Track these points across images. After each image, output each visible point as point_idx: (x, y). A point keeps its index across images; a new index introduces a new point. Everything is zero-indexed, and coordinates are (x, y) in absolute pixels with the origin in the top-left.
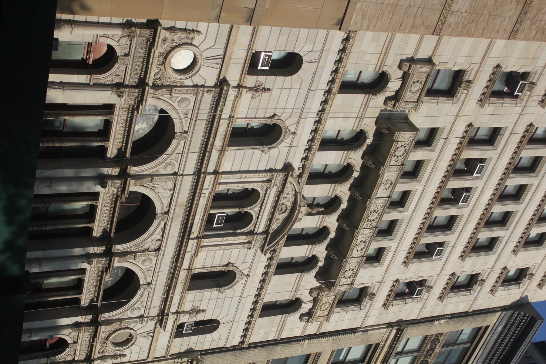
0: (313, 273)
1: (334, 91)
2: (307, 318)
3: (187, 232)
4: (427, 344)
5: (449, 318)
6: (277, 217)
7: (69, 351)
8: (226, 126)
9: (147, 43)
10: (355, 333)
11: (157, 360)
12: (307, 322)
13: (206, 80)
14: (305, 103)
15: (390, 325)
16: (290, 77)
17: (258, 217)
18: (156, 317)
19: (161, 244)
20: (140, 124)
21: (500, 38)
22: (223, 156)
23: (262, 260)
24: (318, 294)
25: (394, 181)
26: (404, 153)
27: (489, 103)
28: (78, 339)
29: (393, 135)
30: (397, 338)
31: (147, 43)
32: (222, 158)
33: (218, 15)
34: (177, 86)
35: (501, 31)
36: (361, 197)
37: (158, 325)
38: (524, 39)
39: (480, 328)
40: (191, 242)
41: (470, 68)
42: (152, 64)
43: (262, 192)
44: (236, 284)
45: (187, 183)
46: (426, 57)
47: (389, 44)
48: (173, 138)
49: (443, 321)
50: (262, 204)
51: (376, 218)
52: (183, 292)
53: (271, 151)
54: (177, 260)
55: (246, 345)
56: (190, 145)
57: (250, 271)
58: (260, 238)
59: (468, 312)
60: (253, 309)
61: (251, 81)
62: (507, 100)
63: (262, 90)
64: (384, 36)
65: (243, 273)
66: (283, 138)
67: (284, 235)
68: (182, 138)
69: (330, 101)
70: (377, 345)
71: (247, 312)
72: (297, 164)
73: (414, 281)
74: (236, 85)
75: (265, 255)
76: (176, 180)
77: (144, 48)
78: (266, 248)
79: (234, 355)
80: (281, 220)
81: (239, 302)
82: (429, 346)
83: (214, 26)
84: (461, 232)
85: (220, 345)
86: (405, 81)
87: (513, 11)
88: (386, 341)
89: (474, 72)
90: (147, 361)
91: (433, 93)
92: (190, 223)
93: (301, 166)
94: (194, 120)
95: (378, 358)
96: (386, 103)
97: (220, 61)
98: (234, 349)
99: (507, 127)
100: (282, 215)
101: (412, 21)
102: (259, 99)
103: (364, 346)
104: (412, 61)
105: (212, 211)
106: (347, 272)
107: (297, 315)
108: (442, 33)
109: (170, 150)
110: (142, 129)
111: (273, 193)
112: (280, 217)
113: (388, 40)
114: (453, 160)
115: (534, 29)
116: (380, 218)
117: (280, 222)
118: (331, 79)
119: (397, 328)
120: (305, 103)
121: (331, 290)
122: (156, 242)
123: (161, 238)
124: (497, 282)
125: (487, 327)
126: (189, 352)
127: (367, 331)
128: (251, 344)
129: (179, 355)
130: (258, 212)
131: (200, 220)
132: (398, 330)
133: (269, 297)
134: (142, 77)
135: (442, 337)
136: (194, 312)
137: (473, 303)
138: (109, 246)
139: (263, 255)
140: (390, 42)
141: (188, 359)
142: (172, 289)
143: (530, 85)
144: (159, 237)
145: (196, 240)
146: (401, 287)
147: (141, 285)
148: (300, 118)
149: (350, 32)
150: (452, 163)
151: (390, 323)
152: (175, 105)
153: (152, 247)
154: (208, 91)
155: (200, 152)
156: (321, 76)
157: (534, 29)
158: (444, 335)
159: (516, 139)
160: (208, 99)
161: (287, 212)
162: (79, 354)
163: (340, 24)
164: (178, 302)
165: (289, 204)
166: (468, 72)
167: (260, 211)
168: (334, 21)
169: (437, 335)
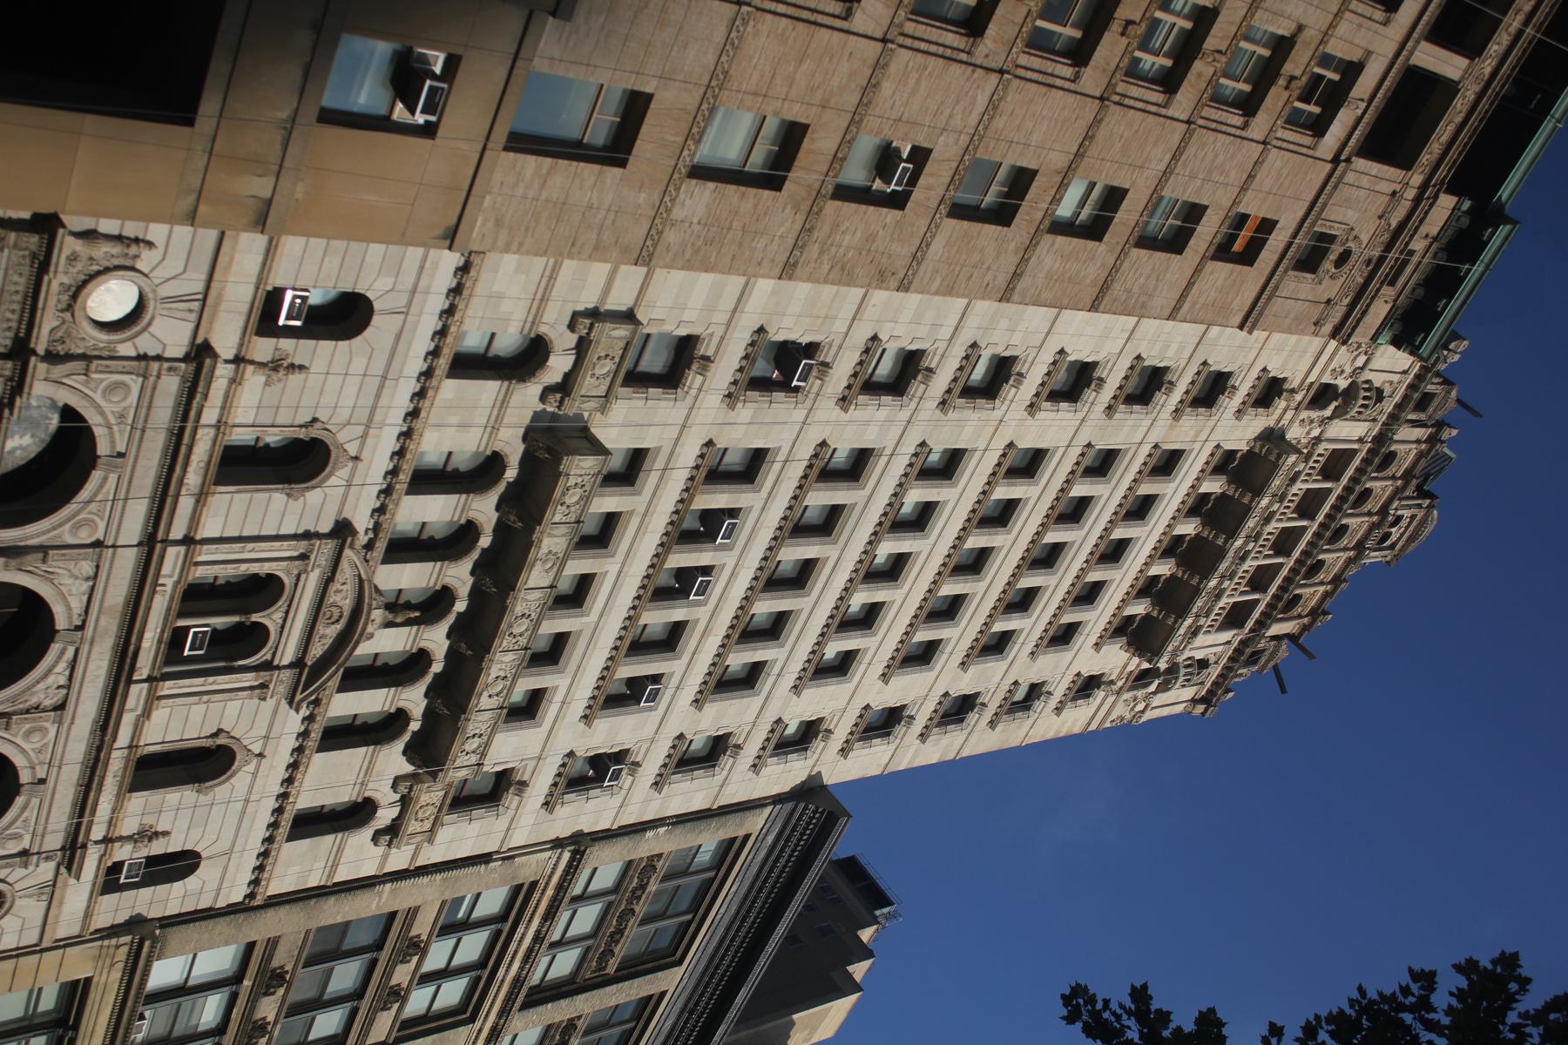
0: (400, 745)
1: (438, 372)
2: (388, 838)
4: (632, 877)
5: (673, 824)
6: (321, 632)
8: (210, 443)
9: (33, 263)
10: (487, 863)
11: (62, 943)
12: (389, 845)
13: (165, 345)
14: (378, 396)
15: (558, 844)
16: (346, 343)
17: (281, 633)
18: (59, 853)
19: (67, 694)
20: (16, 437)
21: (763, 276)
22: (204, 505)
23: (293, 722)
24: (411, 788)
25: (561, 555)
26: (581, 498)
27: (745, 401)
29: (559, 461)
30: (572, 869)
31: (33, 263)
32: (202, 510)
33: (192, 209)
34: (100, 358)
35: (765, 263)
37: (63, 870)
38: (808, 280)
39: (734, 839)
40: (134, 689)
41: (708, 331)
42: (44, 309)
43: (288, 581)
44: (235, 773)
45: (125, 565)
46: (624, 308)
47: (549, 281)
48: (93, 466)
49: (662, 830)
51: (527, 630)
52: (118, 796)
53: (308, 494)
54: (104, 728)
55: (259, 901)
57: (265, 745)
58: (287, 675)
59: (709, 810)
60: (274, 825)
61: (263, 348)
62: (779, 396)
63: (287, 367)
64: (539, 264)
65: (249, 750)
66: (333, 468)
67: (337, 670)
68: (112, 467)
69: (430, 393)
70: (534, 885)
71: (261, 832)
72: (362, 521)
73: (605, 753)
74: (231, 357)
75: (297, 711)
78: (298, 697)
81: (244, 812)
82: (636, 880)
83: (183, 232)
84: (694, 654)
87: (787, 225)
88: (550, 877)
89: (715, 340)
90: (38, 948)
91: (637, 379)
92: (132, 648)
93: (371, 526)
94: (140, 429)
95: (534, 911)
97: (196, 306)
98: (233, 910)
99: (780, 448)
100: (333, 627)
101: (594, 236)
102: (280, 386)
103: (508, 887)
104: (595, 314)
105: (181, 623)
107: (367, 833)
108: (653, 262)
109: (87, 493)
110: (21, 448)
111: (313, 580)
112: (328, 633)
113: (547, 273)
114: (676, 512)
115: (826, 262)
117: (328, 641)
118: (431, 348)
119: (572, 848)
120: (378, 396)
123: (67, 683)
124: (763, 748)
125: (747, 837)
126: (135, 924)
127: (512, 857)
128: (270, 897)
129: (113, 931)
130: (280, 621)
131: (155, 642)
132: (574, 853)
133: (307, 798)
134: (21, 335)
135: (661, 863)
136: (143, 837)
137: (719, 791)
139: (293, 712)
140: (552, 277)
143: (821, 368)
144: (62, 680)
145: (146, 685)
146: (578, 767)
147: (23, 785)
148: (368, 426)
149: (470, 253)
150: (675, 517)
151: (558, 839)
152: (98, 397)
153: (48, 703)
154: (170, 369)
155: (153, 498)
156: (410, 344)
157: (826, 262)
158: (664, 856)
159: (796, 470)
160: (171, 385)
161: (343, 621)
163: (451, 237)
165: (347, 604)
166: (704, 339)
167: (285, 620)
168: (439, 231)
169: (651, 858)
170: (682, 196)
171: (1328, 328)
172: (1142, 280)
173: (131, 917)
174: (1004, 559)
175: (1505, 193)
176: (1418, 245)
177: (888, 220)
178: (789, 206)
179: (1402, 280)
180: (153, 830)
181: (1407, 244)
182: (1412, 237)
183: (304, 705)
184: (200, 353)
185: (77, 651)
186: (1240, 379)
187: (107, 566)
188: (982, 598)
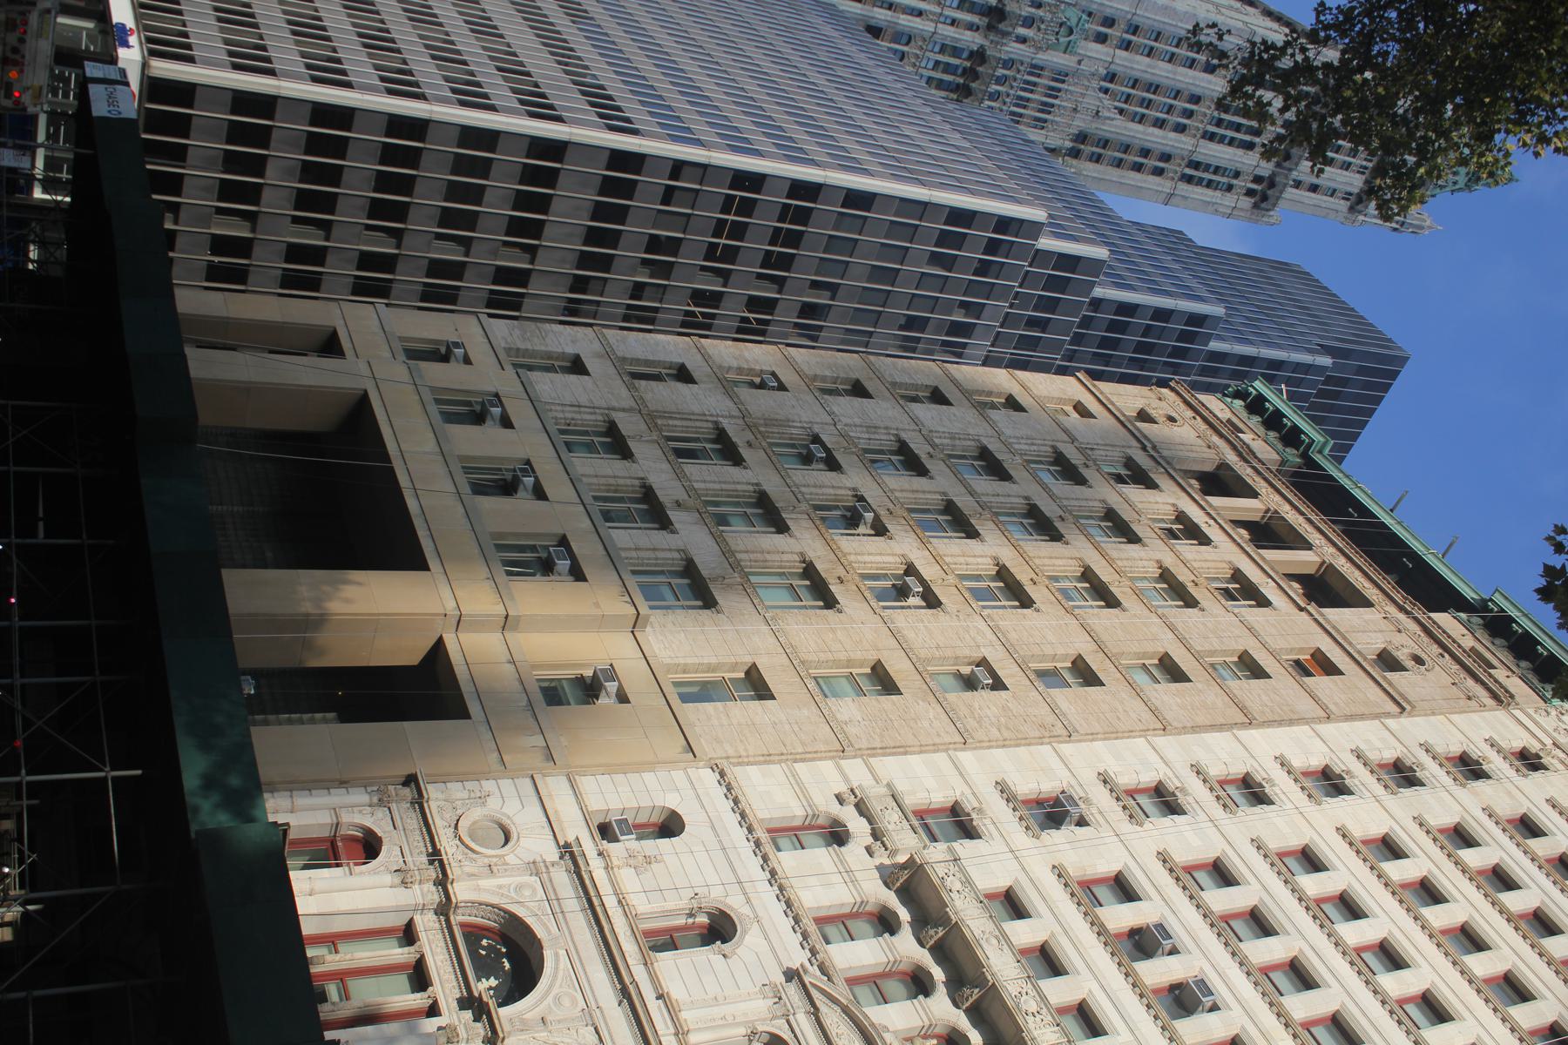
22: (652, 964)
43: (786, 1035)
56: (577, 952)
76: (592, 1017)
77: (414, 815)
83: (506, 784)
93: (719, 777)
110: (490, 988)
113: (789, 774)
116: (1045, 1004)
150: (1096, 929)
170: (833, 708)
171: (1490, 702)
172: (1264, 698)
174: (1493, 928)
175: (1469, 594)
176: (1468, 642)
178: (920, 702)
179: (1488, 655)
181: (1464, 651)
182: (1460, 646)
184: (568, 852)
186: (1476, 751)
187: (603, 1025)
188: (1522, 959)
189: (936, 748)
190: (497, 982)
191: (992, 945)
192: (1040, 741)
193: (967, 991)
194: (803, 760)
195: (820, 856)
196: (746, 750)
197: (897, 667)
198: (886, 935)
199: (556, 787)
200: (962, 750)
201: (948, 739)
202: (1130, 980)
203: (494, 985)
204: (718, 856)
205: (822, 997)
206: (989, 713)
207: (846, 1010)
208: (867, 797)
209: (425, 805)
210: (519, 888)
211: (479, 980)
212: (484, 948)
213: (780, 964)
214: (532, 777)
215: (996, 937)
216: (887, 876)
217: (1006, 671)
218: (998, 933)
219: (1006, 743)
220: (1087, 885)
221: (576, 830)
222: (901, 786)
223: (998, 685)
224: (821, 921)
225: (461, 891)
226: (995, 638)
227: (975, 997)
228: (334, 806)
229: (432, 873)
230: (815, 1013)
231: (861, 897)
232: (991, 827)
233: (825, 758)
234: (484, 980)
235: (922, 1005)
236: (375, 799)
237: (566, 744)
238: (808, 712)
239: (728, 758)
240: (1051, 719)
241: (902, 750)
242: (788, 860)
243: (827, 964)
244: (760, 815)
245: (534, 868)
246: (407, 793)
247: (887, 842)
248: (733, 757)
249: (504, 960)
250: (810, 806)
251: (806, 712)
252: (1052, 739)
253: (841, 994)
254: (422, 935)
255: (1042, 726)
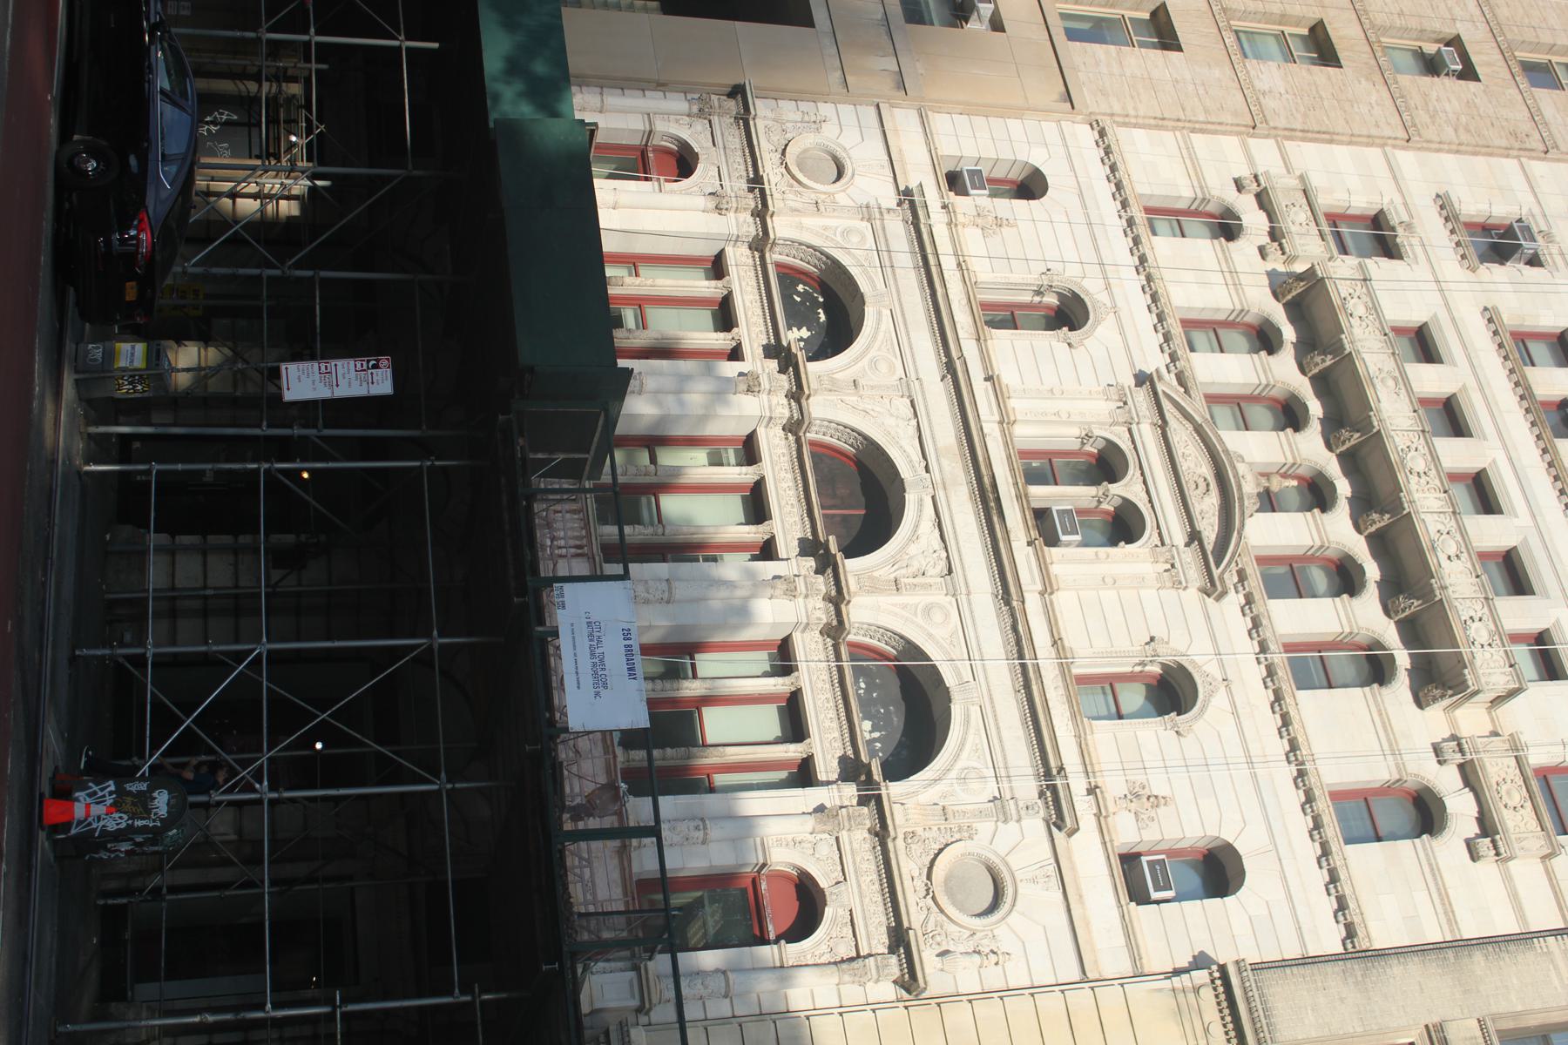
0: (1401, 686)
1: (1257, 596)
3: (992, 504)
7: (834, 920)
17: (1153, 507)
19: (948, 557)
22: (985, 340)
28: (844, 874)
36: (1358, 431)
43: (1125, 445)
50: (1143, 474)
54: (1006, 597)
56: (903, 315)
69: (1308, 766)
77: (737, 132)
78: (1216, 573)
79: (1350, 980)
80: (1214, 515)
81: (1254, 776)
83: (846, 110)
85: (1292, 952)
86: (1270, 208)
92: (986, 480)
96: (1475, 855)
106: (1475, 626)
110: (801, 339)
111: (1148, 436)
112: (1207, 508)
113: (1182, 145)
116: (1435, 465)
121: (1466, 681)
122: (935, 555)
131: (1015, 499)
138: (821, 552)
141: (1211, 974)
142: (1033, 682)
150: (1520, 391)
162: (866, 926)
164: (1081, 768)
165: (1206, 470)
167: (1148, 492)
168: (1055, 96)
170: (1252, 73)
173: (1194, 957)
177: (1473, 90)
178: (1363, 80)
180: (1147, 792)
183: (1226, 576)
184: (907, 197)
185: (933, 498)
189: (1370, 140)
190: (809, 334)
191: (1387, 387)
192: (1506, 152)
193: (1345, 433)
194: (1202, 131)
195: (1203, 248)
196: (1135, 109)
197: (1343, 32)
198: (1263, 353)
199: (903, 120)
200: (1403, 148)
201: (1387, 132)
202: (1548, 457)
203: (805, 337)
204: (1082, 231)
205: (1174, 410)
206: (1448, 108)
207: (1198, 429)
208: (1273, 188)
209: (751, 123)
210: (846, 232)
211: (790, 328)
212: (799, 294)
213: (1133, 364)
214: (878, 106)
215: (1395, 379)
216: (1278, 286)
217: (1484, 56)
218: (1398, 374)
219: (1463, 148)
220: (1522, 339)
221: (921, 175)
222: (1316, 181)
223: (1468, 73)
224: (1189, 324)
225: (781, 227)
226: (1478, 12)
227: (1353, 442)
228: (649, 111)
229: (751, 201)
230: (1163, 426)
231: (1242, 304)
232: (1419, 250)
233: (1230, 133)
234: (795, 329)
235: (1288, 440)
236: (695, 109)
237: (921, 71)
238: (1220, 73)
239: (1112, 115)
240: (1527, 126)
241: (1327, 137)
242: (1163, 247)
243: (1186, 374)
244: (1140, 189)
245: (867, 212)
246: (732, 105)
247: (1285, 245)
248: (1119, 115)
249: (820, 311)
250: (1201, 188)
251: (1217, 73)
252: (1522, 153)
253: (1197, 411)
254: (732, 270)
255: (1514, 134)
